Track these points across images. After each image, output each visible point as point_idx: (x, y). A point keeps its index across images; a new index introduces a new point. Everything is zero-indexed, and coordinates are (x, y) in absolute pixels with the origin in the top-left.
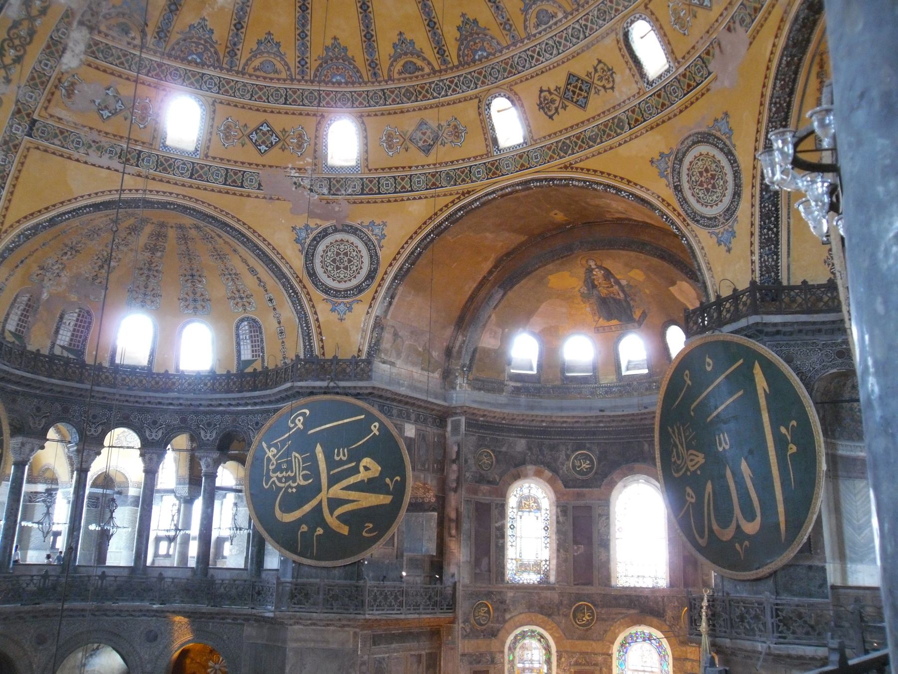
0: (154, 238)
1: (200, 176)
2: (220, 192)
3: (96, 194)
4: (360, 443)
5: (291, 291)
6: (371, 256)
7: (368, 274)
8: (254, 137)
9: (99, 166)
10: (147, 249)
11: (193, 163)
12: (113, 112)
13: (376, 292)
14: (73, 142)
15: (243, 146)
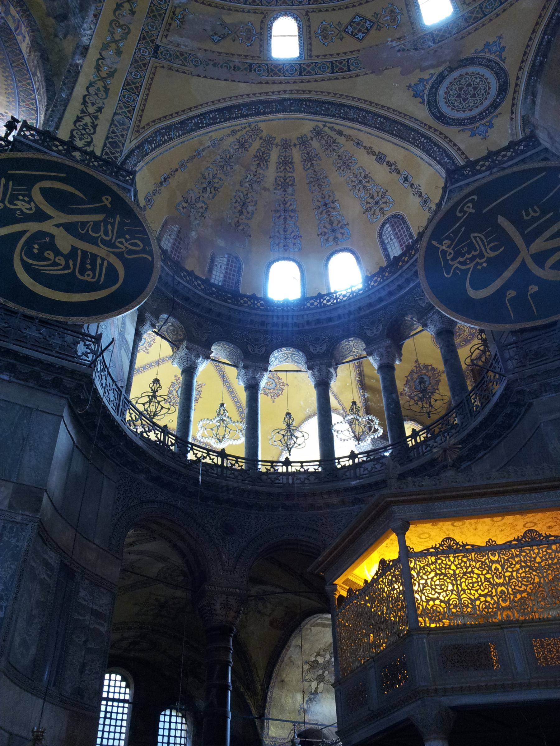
0: (283, 168)
1: (309, 72)
2: (330, 79)
3: (219, 100)
4: (551, 194)
5: (423, 139)
6: (496, 74)
7: (500, 89)
8: (350, 29)
9: (218, 79)
10: (278, 185)
11: (300, 64)
12: (222, 36)
13: (514, 98)
14: (192, 61)
15: (341, 39)
